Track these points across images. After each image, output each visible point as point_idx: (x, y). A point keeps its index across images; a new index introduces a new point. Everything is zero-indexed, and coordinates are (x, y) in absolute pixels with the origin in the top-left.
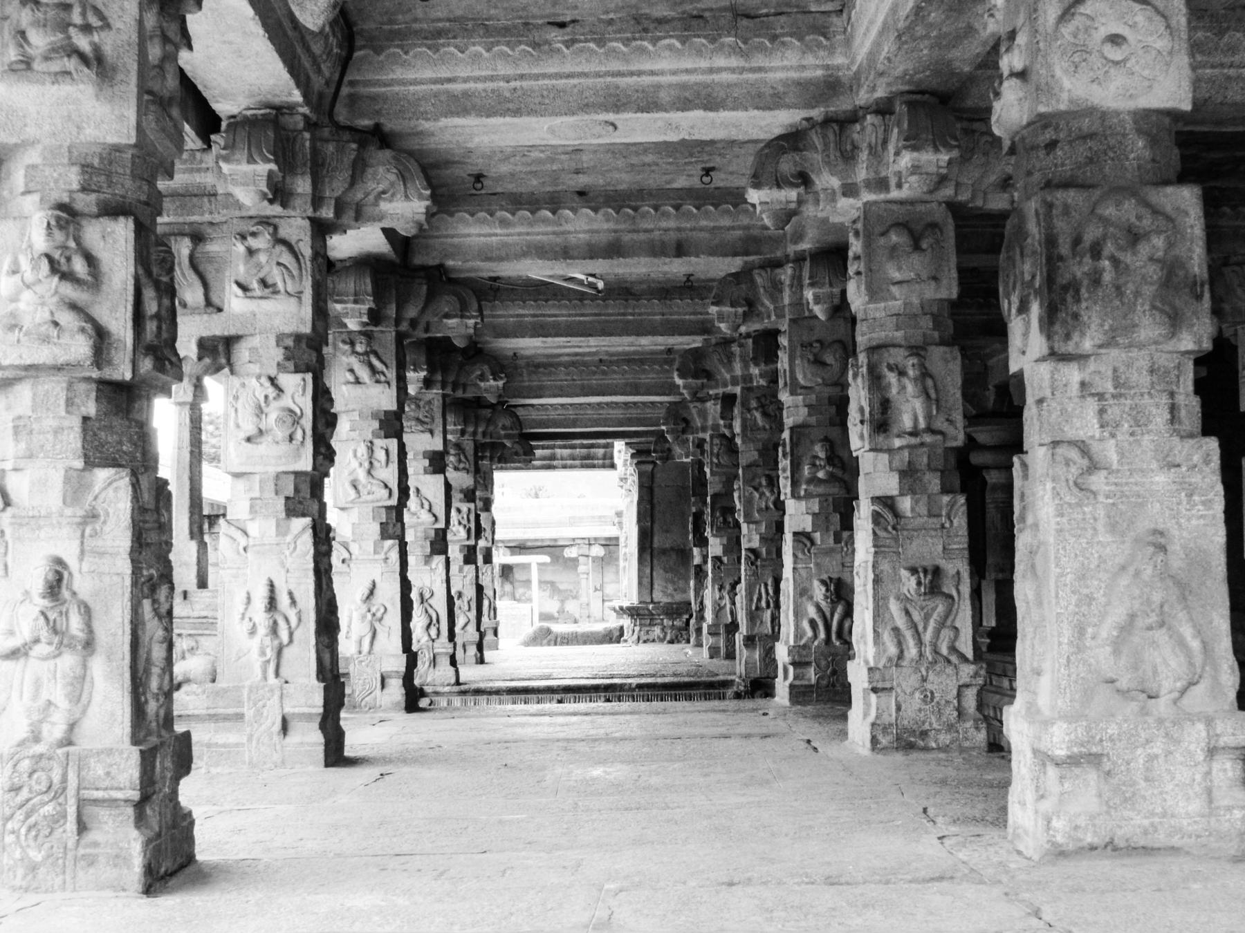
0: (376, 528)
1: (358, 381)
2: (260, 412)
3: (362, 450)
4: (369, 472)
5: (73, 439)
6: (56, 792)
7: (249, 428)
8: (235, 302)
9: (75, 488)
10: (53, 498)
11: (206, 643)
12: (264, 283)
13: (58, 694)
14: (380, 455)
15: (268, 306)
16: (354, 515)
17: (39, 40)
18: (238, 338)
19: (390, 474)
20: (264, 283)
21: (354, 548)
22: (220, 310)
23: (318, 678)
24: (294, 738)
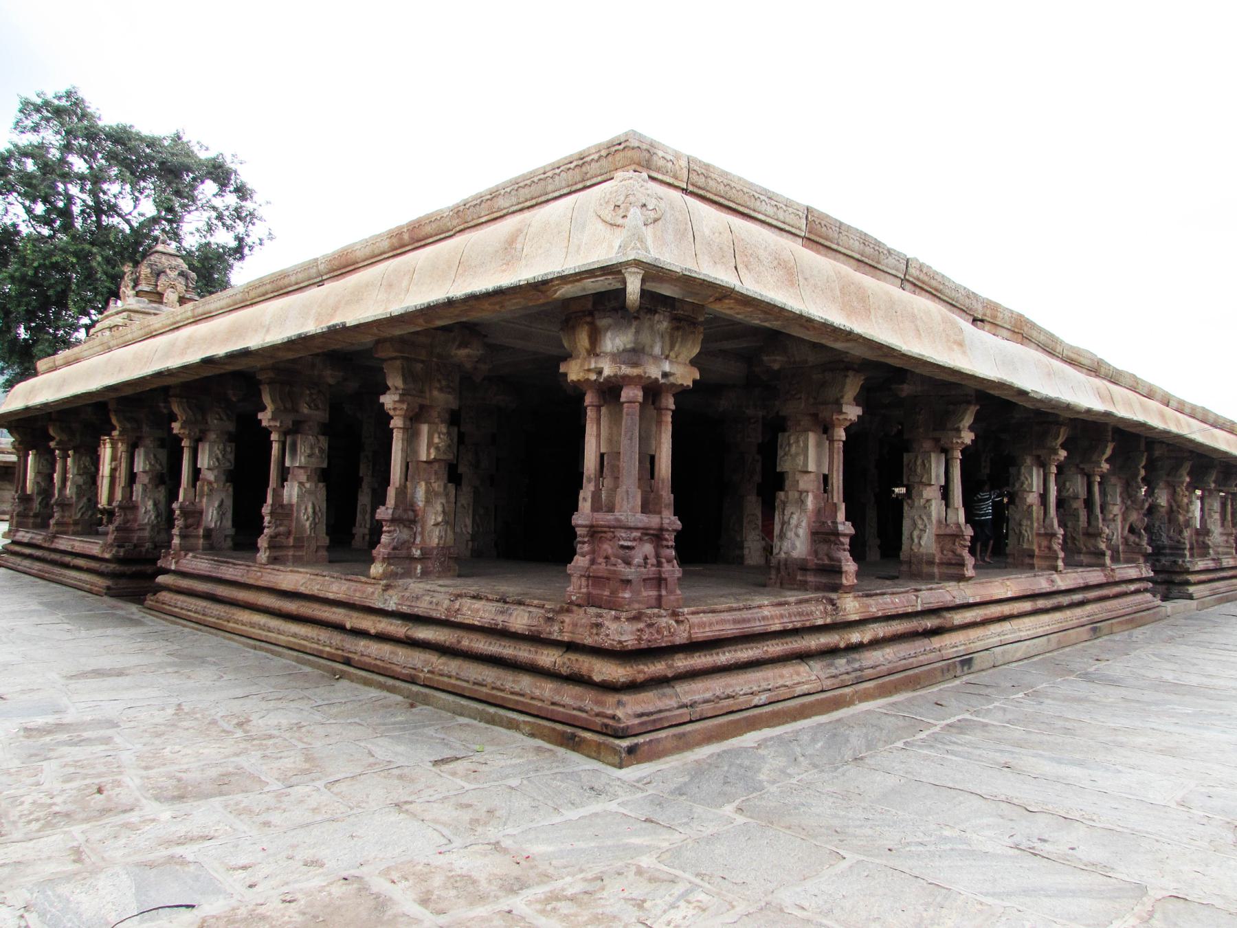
0: (223, 478)
1: (221, 419)
2: (312, 448)
3: (221, 447)
4: (223, 456)
5: (446, 476)
6: (444, 555)
7: (308, 451)
8: (305, 410)
9: (445, 487)
10: (441, 490)
11: (286, 522)
12: (316, 405)
13: (443, 533)
14: (229, 449)
15: (316, 412)
16: (216, 472)
17: (444, 383)
18: (305, 422)
19: (231, 457)
20: (316, 405)
21: (215, 486)
22: (297, 411)
23: (327, 534)
24: (320, 553)
